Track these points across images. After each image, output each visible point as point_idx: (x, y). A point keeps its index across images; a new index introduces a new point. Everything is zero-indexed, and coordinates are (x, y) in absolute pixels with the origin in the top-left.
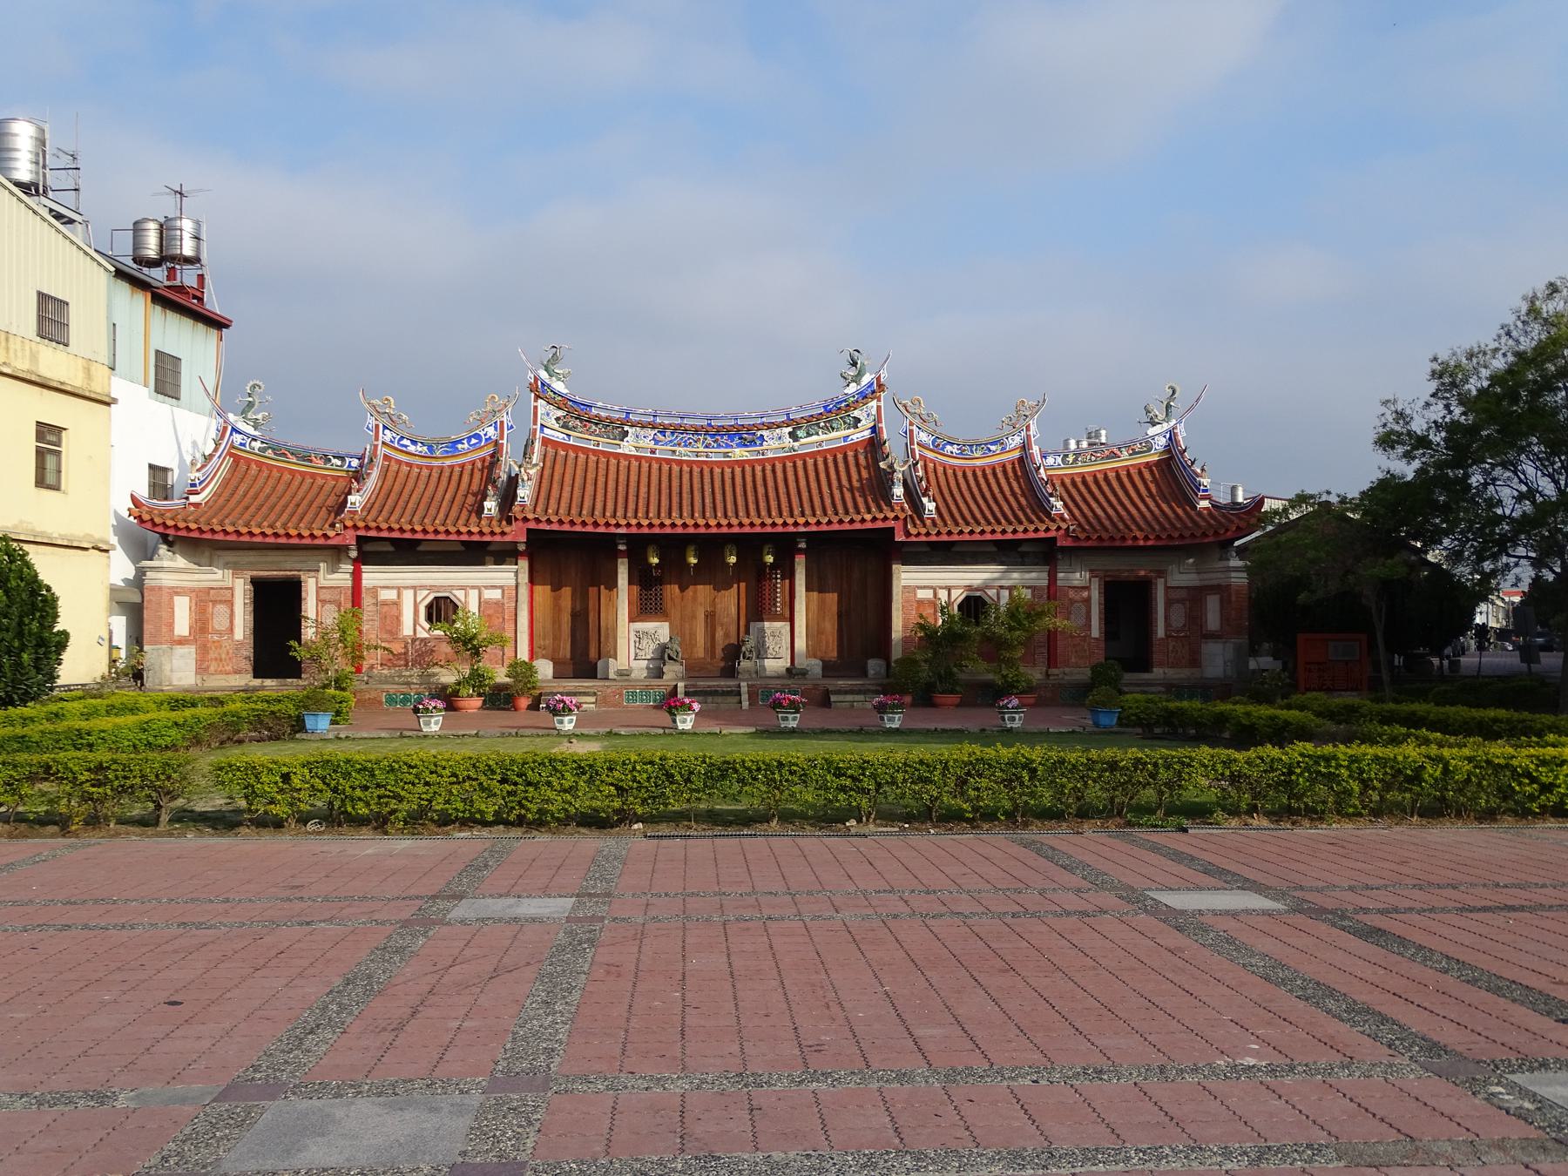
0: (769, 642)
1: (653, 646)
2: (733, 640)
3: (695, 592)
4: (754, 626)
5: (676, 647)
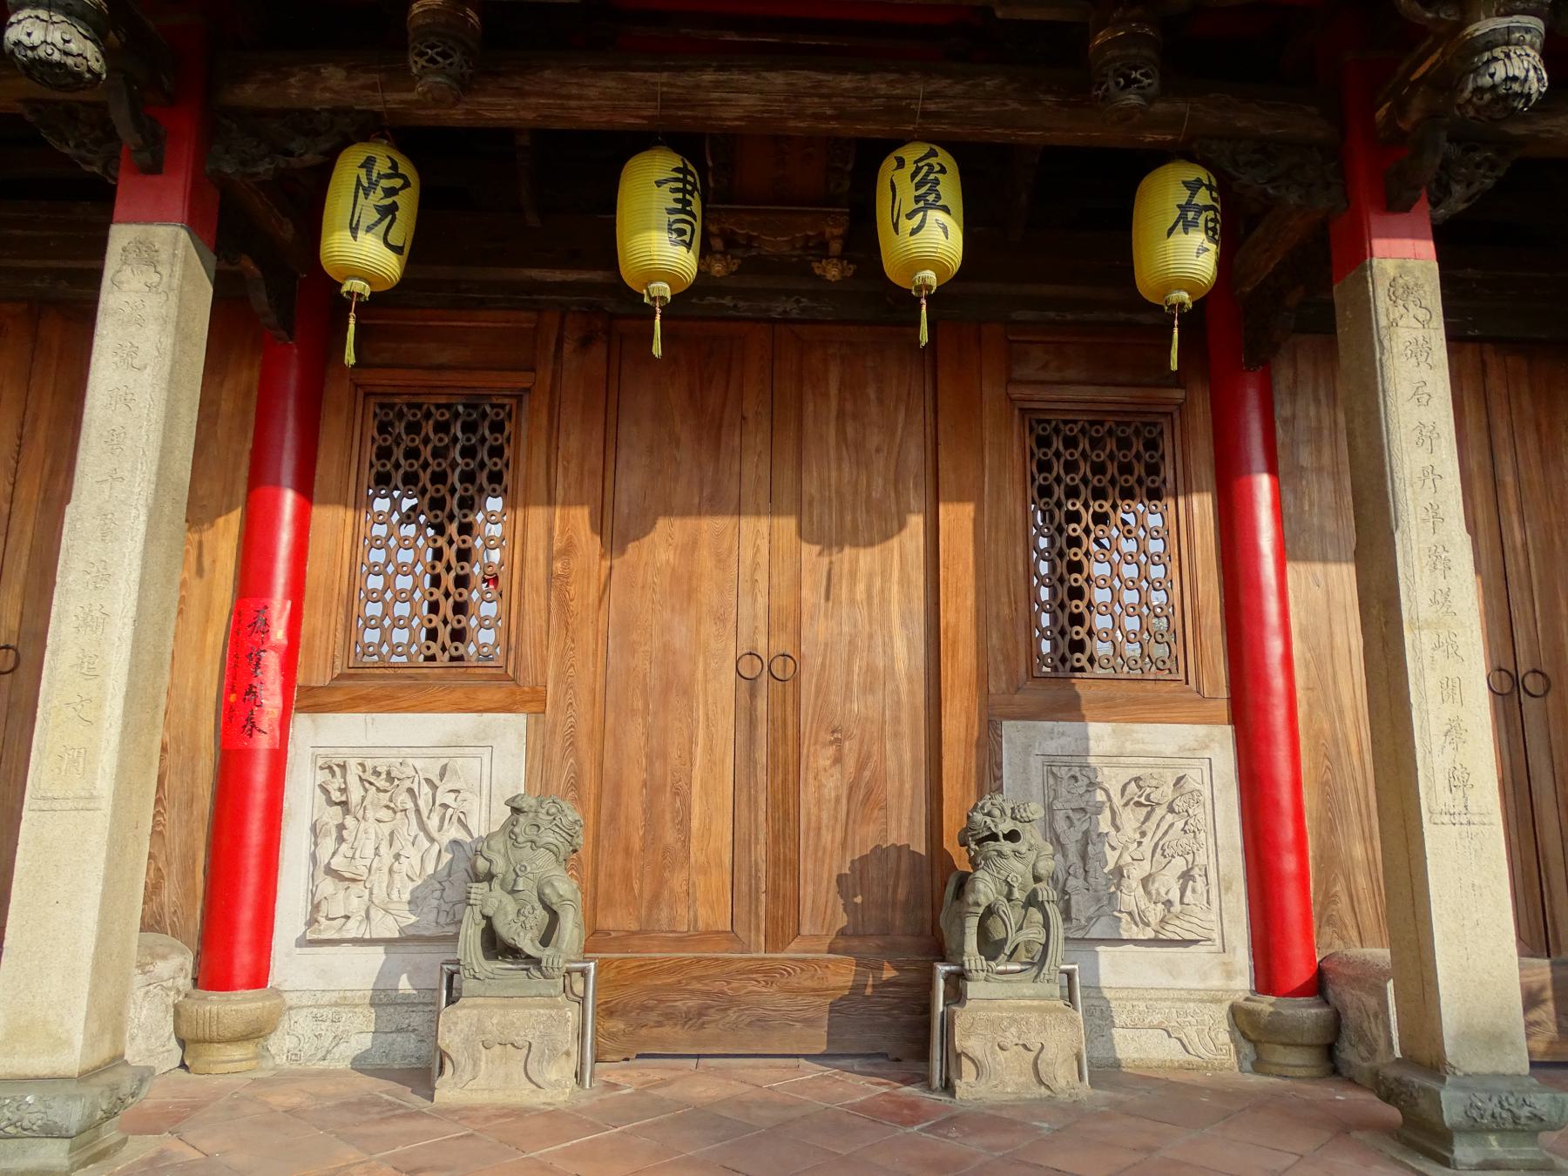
0: (1124, 840)
1: (420, 859)
2: (905, 829)
3: (690, 547)
4: (1027, 744)
5: (543, 864)
